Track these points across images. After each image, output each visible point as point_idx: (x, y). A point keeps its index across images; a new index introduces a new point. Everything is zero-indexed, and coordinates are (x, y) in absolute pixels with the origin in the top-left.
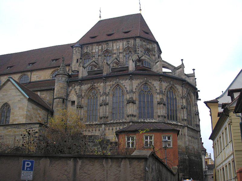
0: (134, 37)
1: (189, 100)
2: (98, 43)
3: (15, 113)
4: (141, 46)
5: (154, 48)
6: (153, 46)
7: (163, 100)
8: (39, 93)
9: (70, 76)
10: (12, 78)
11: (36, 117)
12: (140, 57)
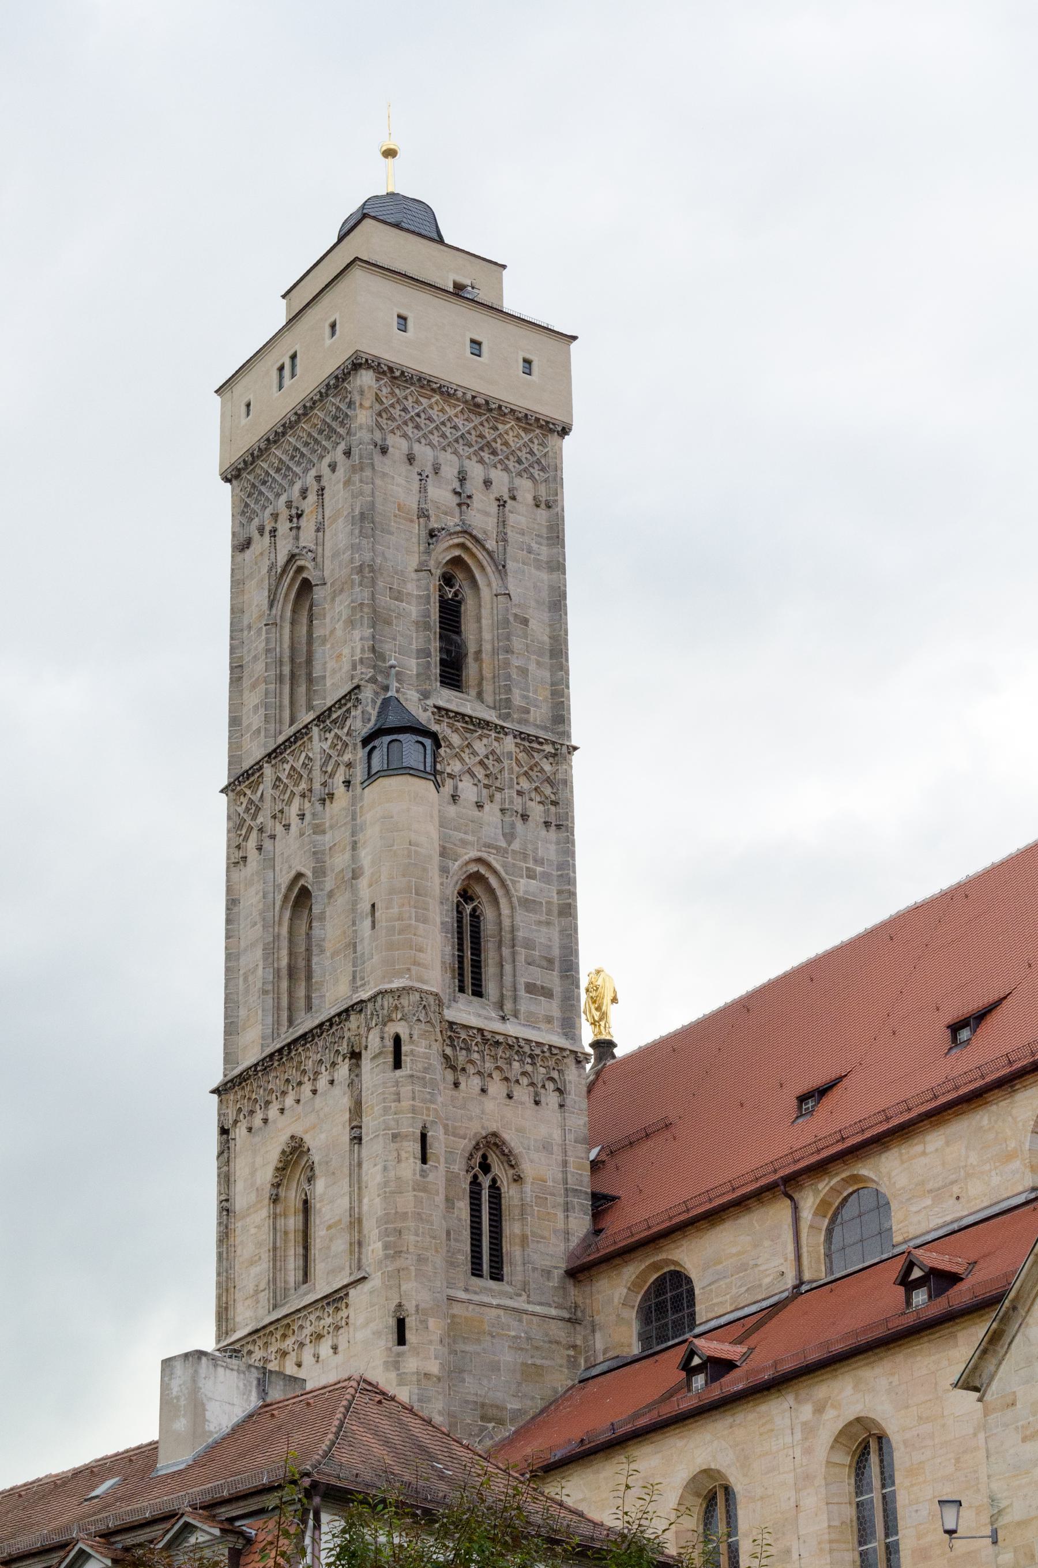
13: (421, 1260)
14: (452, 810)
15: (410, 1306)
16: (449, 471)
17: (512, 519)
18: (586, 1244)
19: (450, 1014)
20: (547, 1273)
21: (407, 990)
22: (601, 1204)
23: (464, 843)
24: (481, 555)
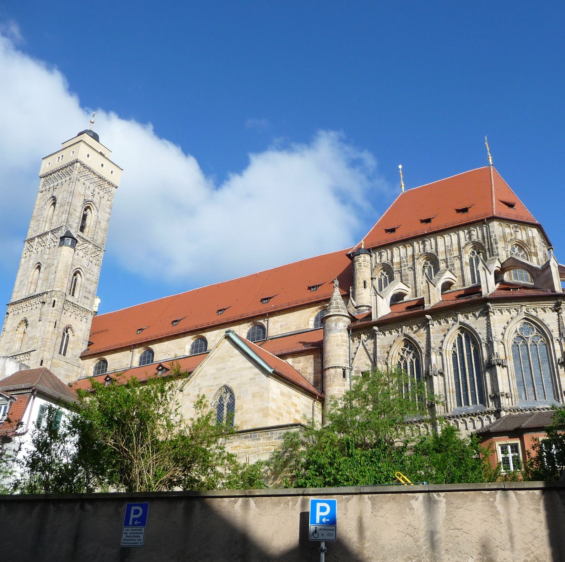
0: (483, 220)
2: (406, 241)
3: (245, 406)
4: (500, 236)
5: (531, 240)
6: (530, 235)
8: (290, 361)
10: (233, 332)
11: (289, 413)
12: (502, 262)
13: (50, 348)
14: (76, 257)
15: (45, 358)
16: (91, 189)
17: (102, 202)
18: (85, 352)
19: (67, 298)
20: (76, 356)
21: (59, 291)
22: (90, 344)
23: (77, 264)
24: (94, 207)
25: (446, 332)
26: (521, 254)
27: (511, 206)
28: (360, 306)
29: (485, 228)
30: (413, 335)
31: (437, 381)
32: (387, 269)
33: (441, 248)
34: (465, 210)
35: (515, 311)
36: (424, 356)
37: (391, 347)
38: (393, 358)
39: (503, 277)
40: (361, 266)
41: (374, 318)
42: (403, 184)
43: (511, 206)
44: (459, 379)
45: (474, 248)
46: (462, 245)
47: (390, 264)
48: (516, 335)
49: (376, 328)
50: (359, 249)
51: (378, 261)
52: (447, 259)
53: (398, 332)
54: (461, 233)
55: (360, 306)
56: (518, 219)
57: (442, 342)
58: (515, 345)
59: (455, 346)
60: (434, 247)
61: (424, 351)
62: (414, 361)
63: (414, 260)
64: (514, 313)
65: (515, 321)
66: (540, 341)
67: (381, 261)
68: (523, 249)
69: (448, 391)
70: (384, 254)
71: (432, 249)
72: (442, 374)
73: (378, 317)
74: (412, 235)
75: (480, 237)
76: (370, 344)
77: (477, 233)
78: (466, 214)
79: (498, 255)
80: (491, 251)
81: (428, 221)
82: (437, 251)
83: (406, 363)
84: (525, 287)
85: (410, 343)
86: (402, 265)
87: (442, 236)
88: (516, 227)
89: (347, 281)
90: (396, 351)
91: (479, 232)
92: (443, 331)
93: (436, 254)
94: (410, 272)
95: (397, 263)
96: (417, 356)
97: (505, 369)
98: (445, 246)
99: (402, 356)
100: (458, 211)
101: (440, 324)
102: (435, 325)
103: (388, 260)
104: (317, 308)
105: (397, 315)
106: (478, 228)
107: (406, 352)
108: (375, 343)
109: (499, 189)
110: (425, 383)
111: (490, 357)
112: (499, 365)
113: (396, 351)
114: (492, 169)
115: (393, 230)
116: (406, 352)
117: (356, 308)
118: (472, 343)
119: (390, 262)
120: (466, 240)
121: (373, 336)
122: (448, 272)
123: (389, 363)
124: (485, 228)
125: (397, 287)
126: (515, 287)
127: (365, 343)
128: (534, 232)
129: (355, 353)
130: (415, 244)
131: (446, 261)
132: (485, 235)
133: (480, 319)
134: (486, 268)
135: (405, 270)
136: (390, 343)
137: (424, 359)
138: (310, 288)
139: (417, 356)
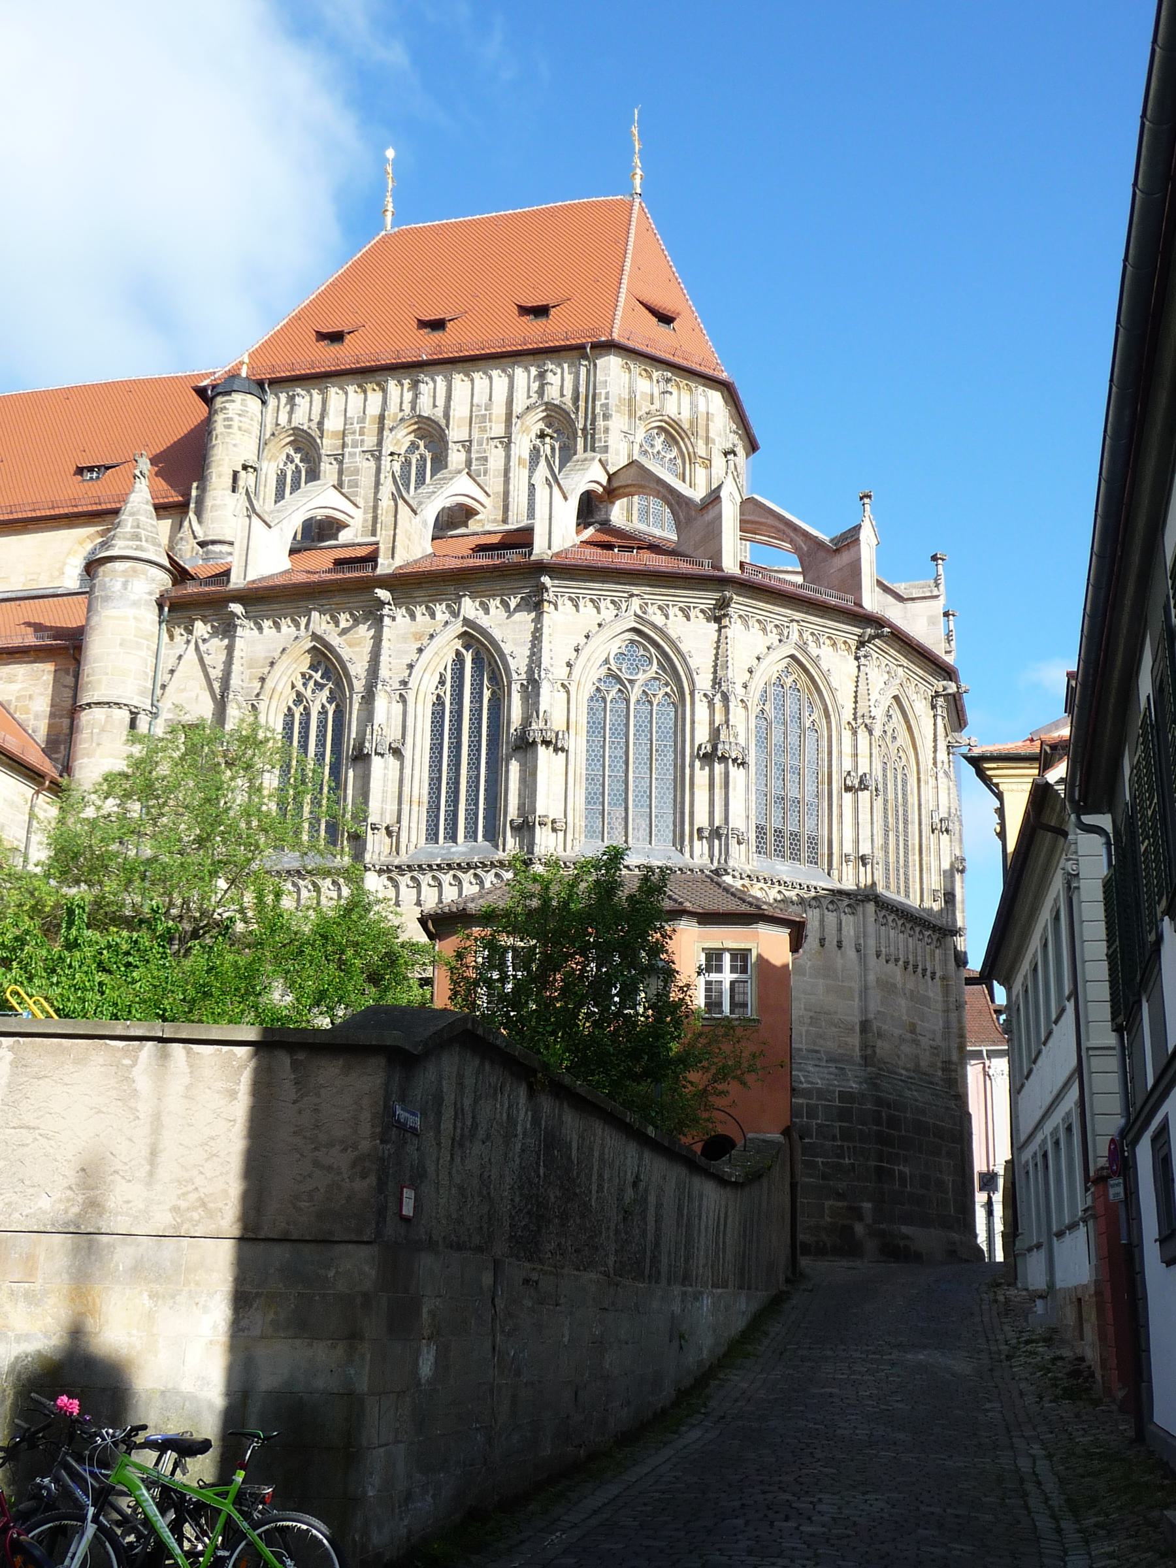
1: (900, 741)
5: (702, 422)
6: (702, 408)
7: (736, 736)
9: (180, 574)
25: (425, 642)
26: (669, 456)
27: (666, 319)
28: (214, 542)
29: (583, 370)
30: (334, 640)
31: (382, 769)
32: (305, 445)
33: (460, 410)
34: (541, 311)
35: (611, 606)
36: (357, 699)
37: (272, 664)
38: (276, 696)
39: (608, 513)
40: (229, 427)
41: (237, 581)
42: (390, 207)
43: (666, 319)
44: (440, 771)
45: (548, 420)
46: (518, 408)
47: (315, 433)
48: (604, 671)
49: (237, 608)
50: (233, 376)
51: (283, 420)
52: (470, 441)
53: (297, 626)
54: (519, 372)
55: (214, 542)
56: (677, 360)
57: (411, 667)
58: (598, 696)
59: (442, 682)
60: (441, 402)
61: (359, 685)
62: (331, 709)
63: (381, 430)
64: (608, 611)
65: (607, 633)
66: (662, 693)
67: (290, 421)
68: (677, 443)
69: (406, 798)
70: (302, 402)
71: (435, 406)
72: (397, 752)
73: (249, 578)
74: (387, 359)
75: (568, 392)
76: (216, 647)
77: (560, 381)
78: (541, 322)
79: (605, 449)
80: (590, 435)
81: (437, 325)
82: (447, 415)
83: (307, 712)
84: (654, 548)
85: (324, 660)
86: (348, 440)
87: (467, 375)
88: (668, 380)
89: (185, 466)
90: (285, 679)
91: (569, 378)
92: (418, 637)
93: (443, 423)
94: (366, 464)
95: (335, 433)
96: (338, 698)
97: (562, 755)
98: (472, 405)
99: (299, 694)
100: (525, 311)
101: (413, 617)
102: (399, 618)
103: (310, 420)
104: (91, 530)
105: (302, 578)
106: (566, 366)
107: (311, 683)
108: (230, 649)
109: (647, 264)
110: (351, 773)
111: (526, 722)
112: (547, 743)
113: (285, 679)
114: (637, 204)
115: (336, 337)
116: (311, 683)
117: (202, 544)
118: (490, 679)
119: (314, 426)
120: (529, 397)
121: (227, 629)
122: (464, 477)
123: (262, 707)
124: (583, 370)
125: (321, 499)
126: (630, 541)
127: (203, 647)
128: (716, 398)
129: (172, 672)
130: (392, 385)
131: (467, 445)
132: (582, 390)
133: (518, 616)
134: (554, 480)
135: (352, 455)
136: (270, 653)
137: (356, 706)
138: (80, 471)
139: (338, 698)
